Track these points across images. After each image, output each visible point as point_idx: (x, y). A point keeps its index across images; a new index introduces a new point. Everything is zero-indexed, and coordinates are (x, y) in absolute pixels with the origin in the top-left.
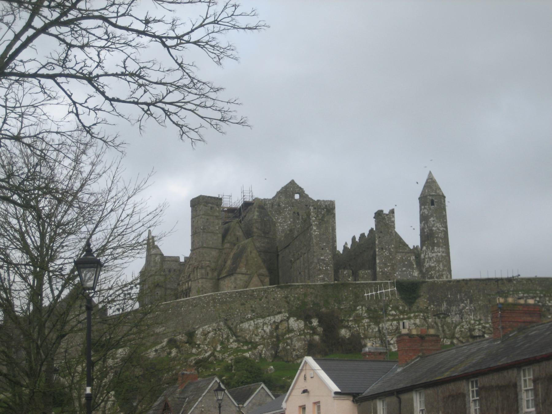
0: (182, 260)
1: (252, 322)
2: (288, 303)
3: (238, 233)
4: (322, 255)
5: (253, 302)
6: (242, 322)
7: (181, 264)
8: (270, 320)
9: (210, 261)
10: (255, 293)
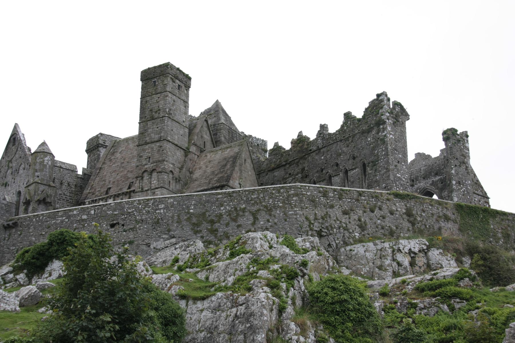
0: (80, 172)
1: (371, 244)
2: (413, 224)
3: (205, 136)
4: (398, 171)
5: (361, 212)
6: (346, 244)
7: (77, 176)
8: (405, 246)
9: (173, 164)
10: (363, 198)
